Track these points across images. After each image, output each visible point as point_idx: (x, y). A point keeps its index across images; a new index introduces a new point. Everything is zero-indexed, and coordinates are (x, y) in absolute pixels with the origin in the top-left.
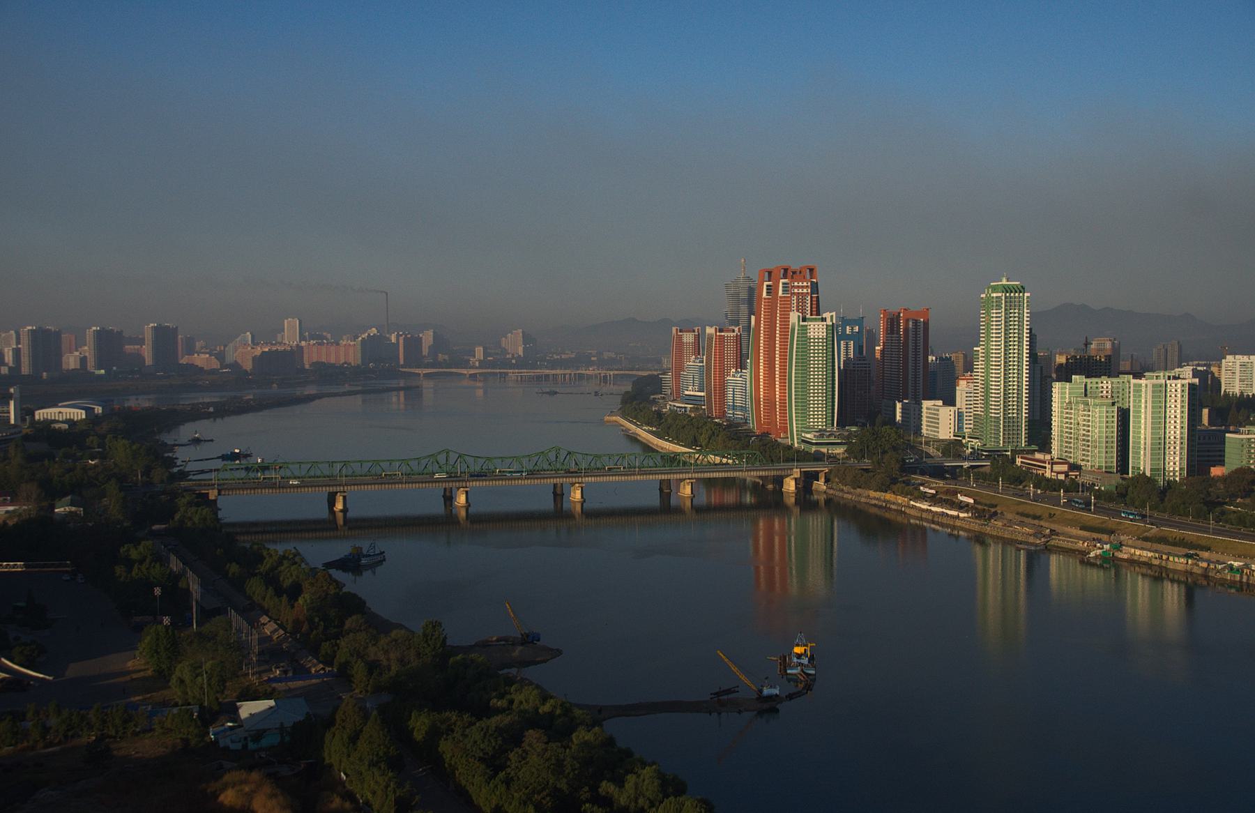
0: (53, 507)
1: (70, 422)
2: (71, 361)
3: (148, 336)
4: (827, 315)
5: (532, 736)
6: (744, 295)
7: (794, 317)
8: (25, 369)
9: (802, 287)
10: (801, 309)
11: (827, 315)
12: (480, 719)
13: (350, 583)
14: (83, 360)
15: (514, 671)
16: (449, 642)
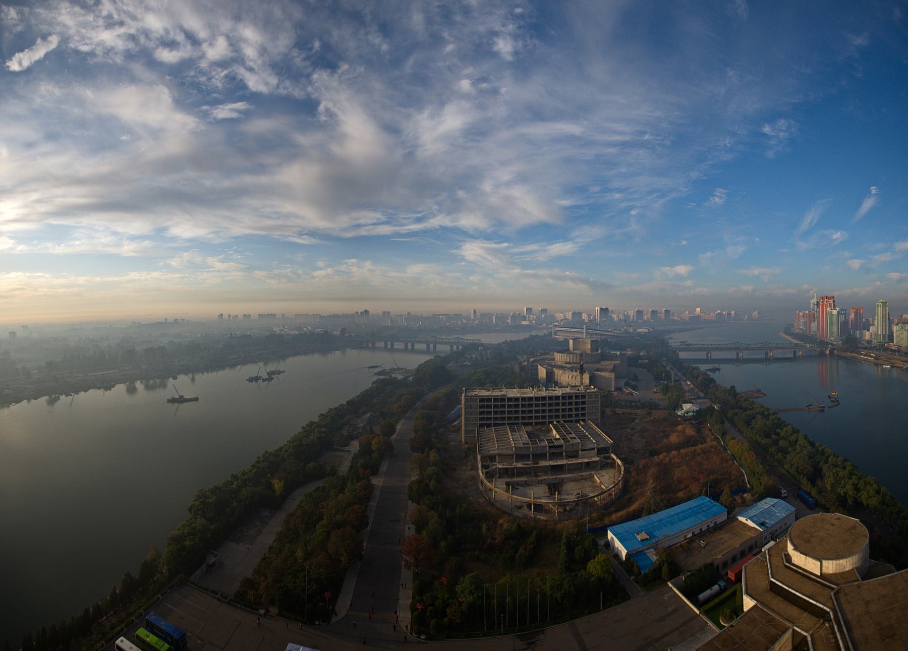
0: (640, 353)
1: (645, 332)
2: (645, 318)
3: (663, 312)
4: (837, 308)
5: (759, 416)
6: (816, 303)
7: (829, 309)
8: (635, 320)
9: (831, 301)
10: (830, 307)
11: (837, 308)
12: (745, 411)
13: (712, 375)
14: (648, 318)
15: (754, 399)
16: (737, 391)
